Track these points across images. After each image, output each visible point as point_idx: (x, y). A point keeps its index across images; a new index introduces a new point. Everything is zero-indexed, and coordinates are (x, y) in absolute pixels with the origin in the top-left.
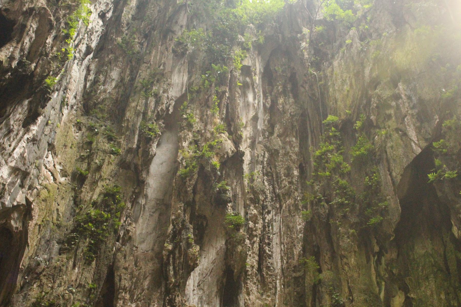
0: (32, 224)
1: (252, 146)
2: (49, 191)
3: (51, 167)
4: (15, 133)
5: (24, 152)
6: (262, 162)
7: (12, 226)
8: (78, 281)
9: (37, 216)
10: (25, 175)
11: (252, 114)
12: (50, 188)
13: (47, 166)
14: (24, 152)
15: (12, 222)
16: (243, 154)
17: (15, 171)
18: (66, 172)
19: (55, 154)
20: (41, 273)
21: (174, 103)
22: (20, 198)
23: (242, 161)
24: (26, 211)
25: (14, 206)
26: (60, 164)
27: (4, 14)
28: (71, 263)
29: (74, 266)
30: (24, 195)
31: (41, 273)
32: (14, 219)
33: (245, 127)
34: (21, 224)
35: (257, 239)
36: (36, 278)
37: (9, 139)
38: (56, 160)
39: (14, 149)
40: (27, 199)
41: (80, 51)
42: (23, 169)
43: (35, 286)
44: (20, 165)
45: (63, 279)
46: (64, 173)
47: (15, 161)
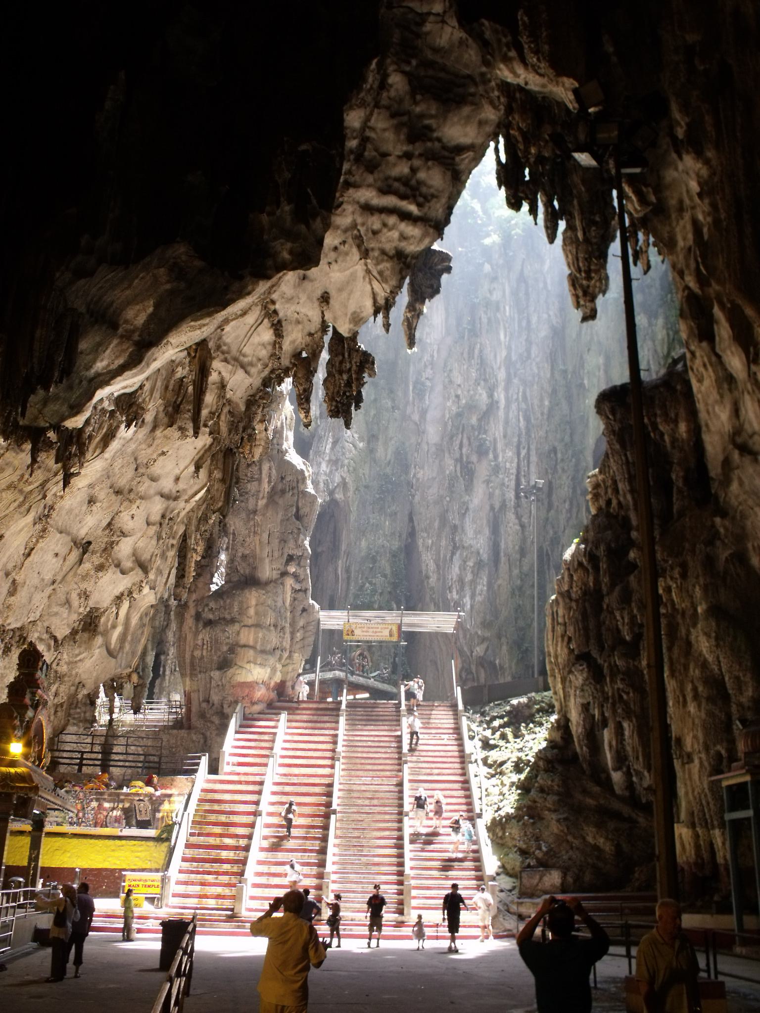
0: (350, 494)
1: (506, 390)
6: (517, 399)
9: (351, 486)
11: (504, 353)
16: (497, 402)
21: (436, 347)
22: (337, 479)
23: (498, 408)
33: (499, 368)
35: (513, 477)
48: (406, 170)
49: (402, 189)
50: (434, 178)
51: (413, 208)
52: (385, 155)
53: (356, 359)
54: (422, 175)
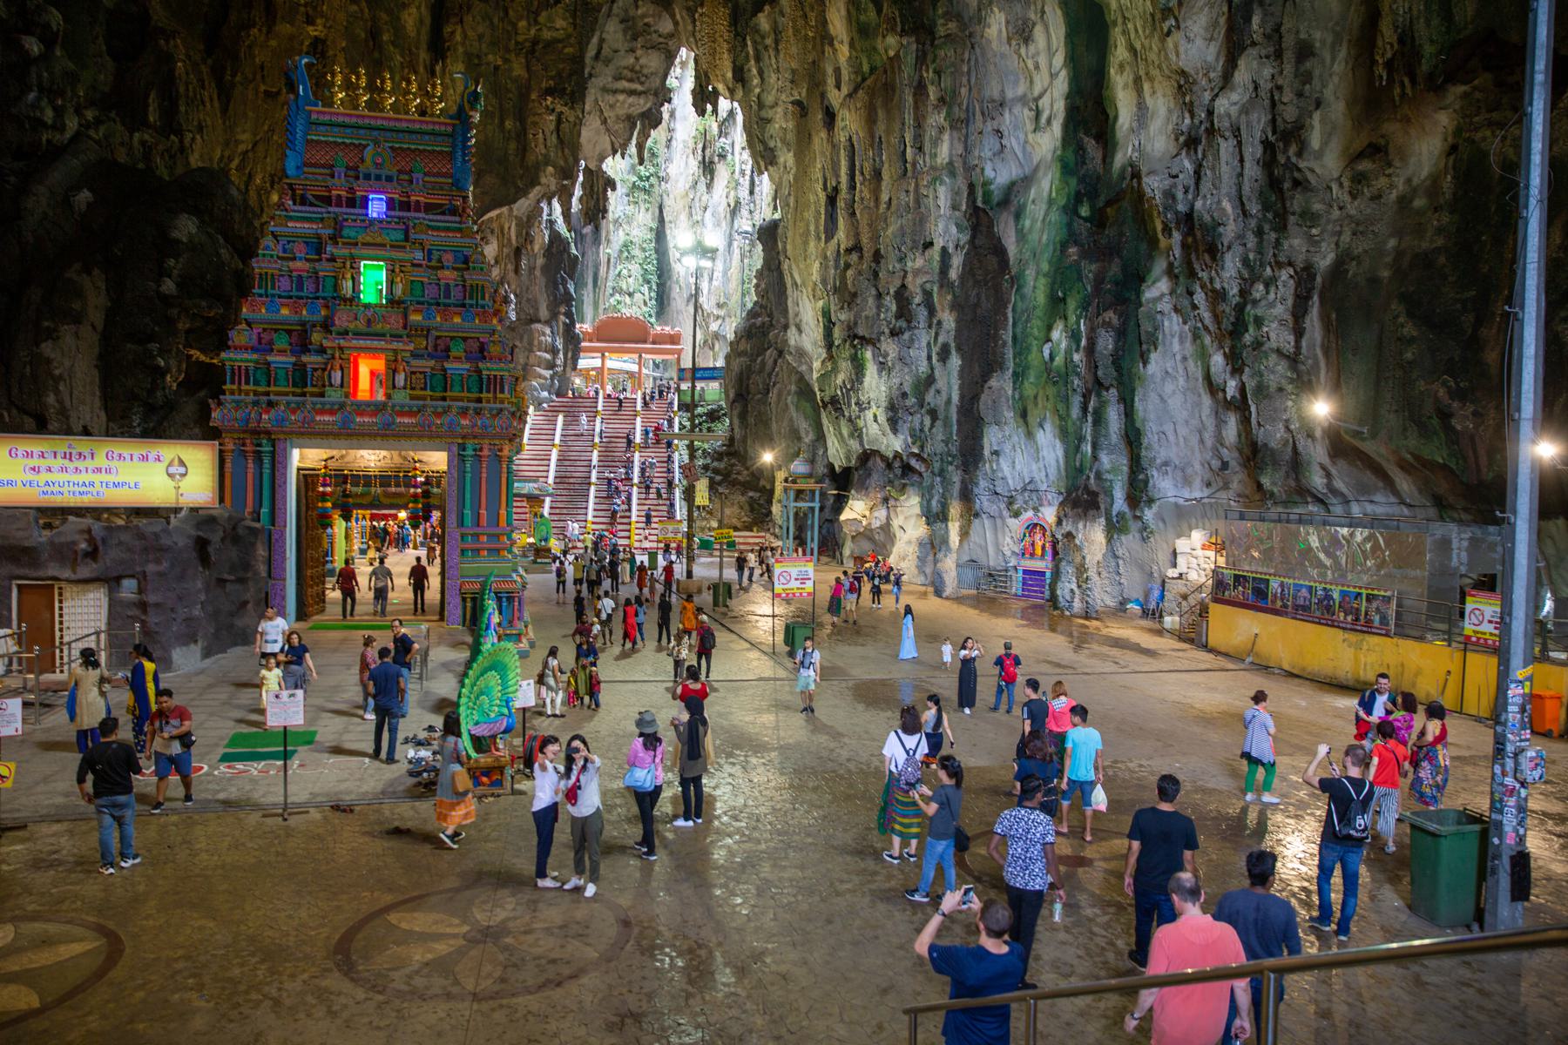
48: (632, 60)
49: (629, 74)
50: (652, 61)
51: (639, 87)
52: (616, 51)
53: (601, 182)
54: (642, 61)
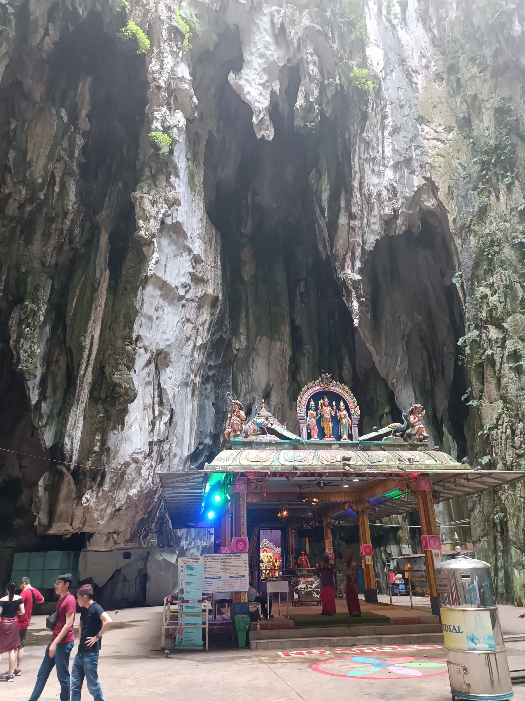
2: (443, 157)
3: (433, 135)
4: (374, 139)
5: (394, 146)
7: (427, 207)
8: (508, 207)
10: (408, 162)
12: (443, 152)
13: (428, 137)
14: (394, 146)
15: (426, 204)
17: (396, 166)
18: (449, 127)
19: (428, 122)
20: (470, 225)
22: (417, 181)
24: (431, 187)
25: (415, 192)
26: (440, 125)
27: (290, 65)
28: (493, 197)
29: (498, 198)
30: (420, 177)
31: (470, 225)
32: (426, 201)
34: (434, 200)
36: (469, 231)
37: (373, 148)
38: (433, 125)
39: (383, 151)
40: (425, 178)
41: (395, 15)
42: (402, 159)
43: (471, 237)
44: (398, 158)
45: (491, 216)
46: (449, 129)
47: (391, 160)
